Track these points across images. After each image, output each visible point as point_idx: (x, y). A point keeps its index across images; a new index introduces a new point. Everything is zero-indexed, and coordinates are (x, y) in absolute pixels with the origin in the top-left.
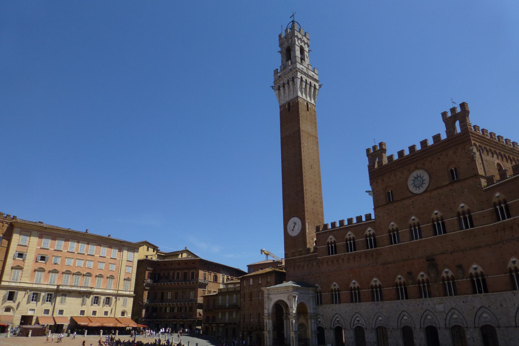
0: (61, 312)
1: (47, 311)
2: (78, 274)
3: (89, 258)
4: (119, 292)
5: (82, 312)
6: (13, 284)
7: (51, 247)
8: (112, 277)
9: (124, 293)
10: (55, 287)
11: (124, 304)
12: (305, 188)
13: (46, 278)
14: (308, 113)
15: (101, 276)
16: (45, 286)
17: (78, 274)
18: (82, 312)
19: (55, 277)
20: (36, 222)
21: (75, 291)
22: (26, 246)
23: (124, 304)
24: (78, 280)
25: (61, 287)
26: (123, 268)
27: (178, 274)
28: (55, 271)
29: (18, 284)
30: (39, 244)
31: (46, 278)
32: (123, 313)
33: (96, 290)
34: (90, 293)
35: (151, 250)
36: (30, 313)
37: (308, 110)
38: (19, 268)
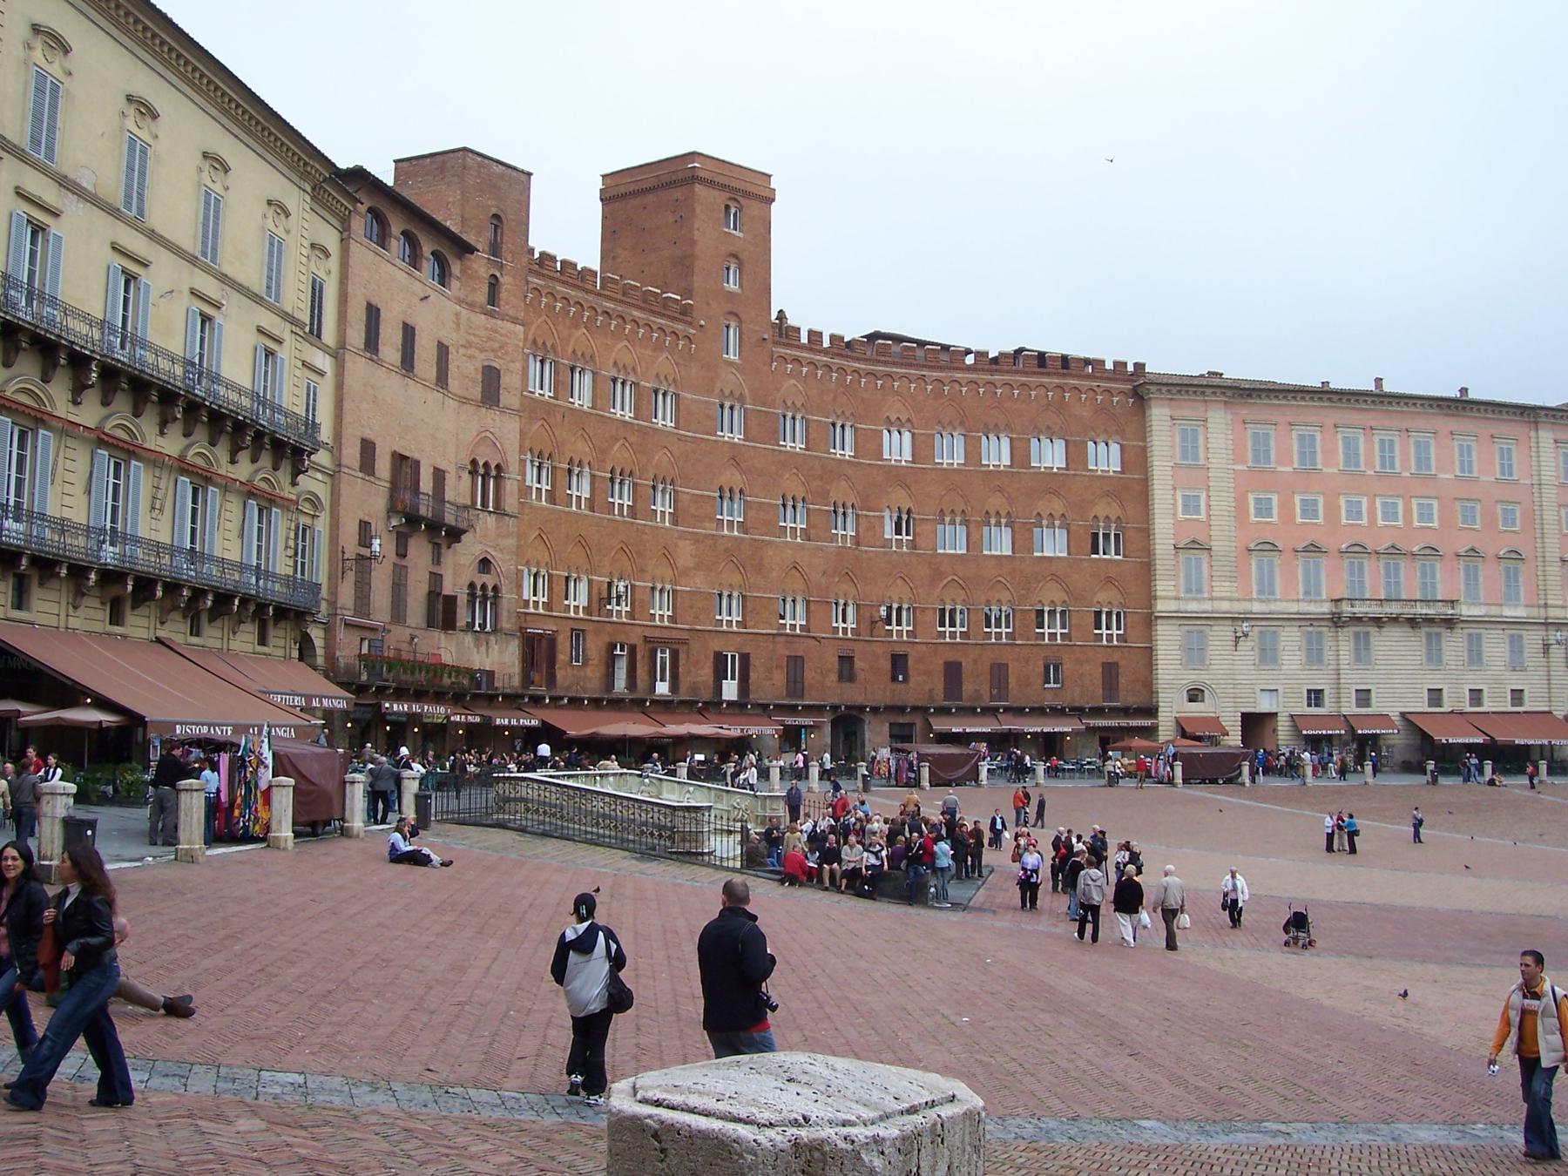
0: (1364, 697)
1: (1315, 697)
2: (1394, 551)
4: (1552, 612)
5: (1435, 696)
6: (1193, 606)
7: (1279, 463)
10: (1326, 608)
16: (1294, 607)
18: (1435, 696)
19: (1317, 573)
20: (1202, 376)
21: (1395, 620)
22: (1202, 467)
24: (1397, 575)
25: (1346, 609)
26: (1550, 516)
28: (1314, 549)
29: (1207, 606)
30: (1238, 457)
33: (1465, 611)
34: (1450, 623)
36: (1264, 705)
38: (1197, 546)
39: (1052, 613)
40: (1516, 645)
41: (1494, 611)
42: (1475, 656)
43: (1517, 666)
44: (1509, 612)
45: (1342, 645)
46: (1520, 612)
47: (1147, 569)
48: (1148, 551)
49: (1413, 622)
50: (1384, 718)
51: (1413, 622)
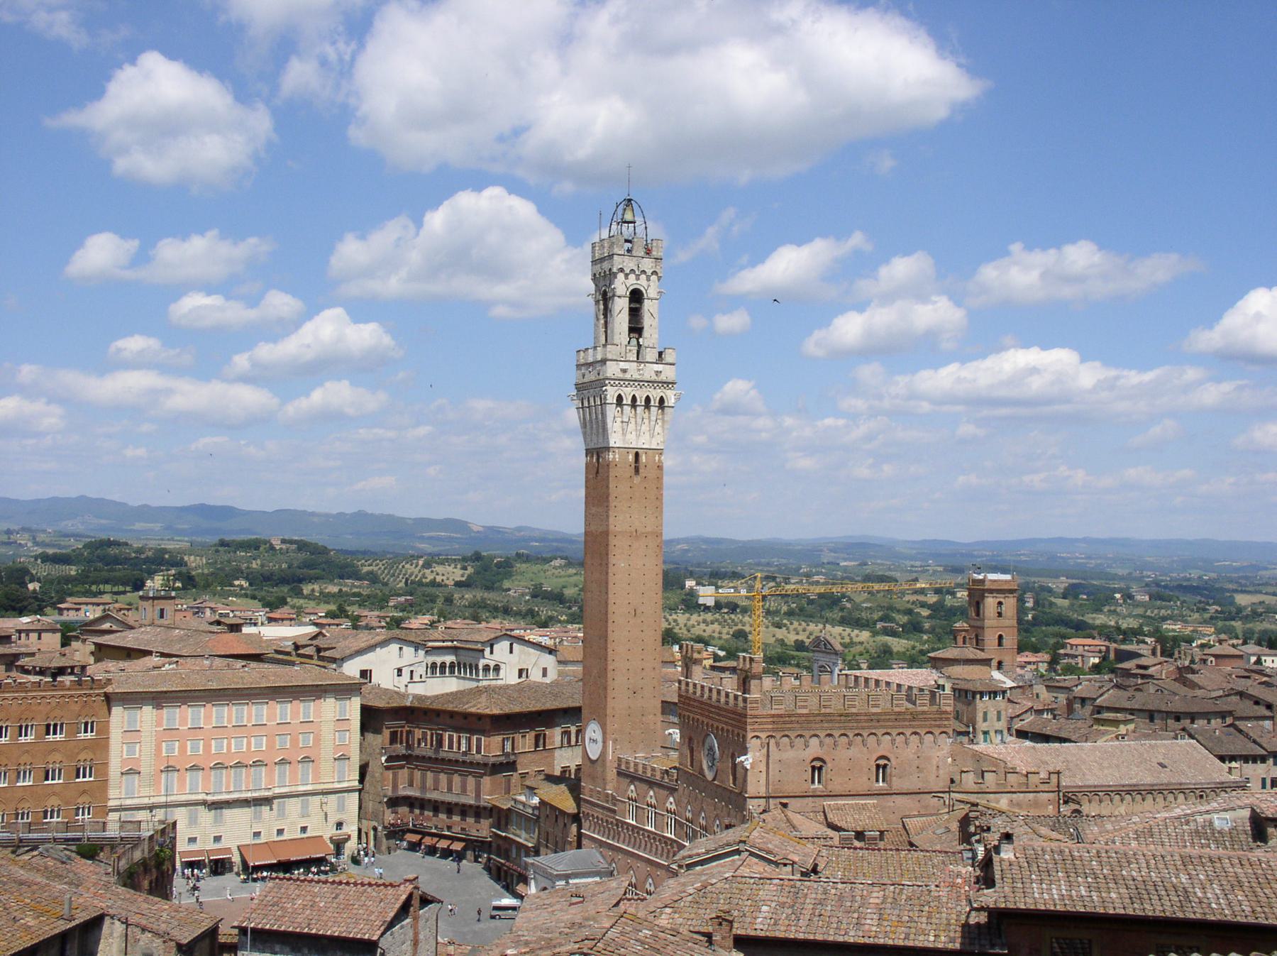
2: (239, 765)
3: (257, 731)
8: (307, 760)
9: (337, 786)
11: (341, 807)
12: (610, 667)
13: (182, 782)
14: (637, 480)
15: (283, 762)
17: (239, 765)
23: (341, 807)
27: (451, 738)
30: (159, 724)
31: (182, 782)
32: (339, 825)
34: (267, 801)
35: (408, 651)
37: (637, 470)
39: (52, 811)
40: (305, 806)
41: (293, 789)
42: (282, 814)
43: (305, 815)
44: (302, 788)
45: (205, 816)
46: (309, 788)
47: (103, 784)
48: (106, 774)
49: (246, 803)
50: (228, 850)
51: (246, 803)
